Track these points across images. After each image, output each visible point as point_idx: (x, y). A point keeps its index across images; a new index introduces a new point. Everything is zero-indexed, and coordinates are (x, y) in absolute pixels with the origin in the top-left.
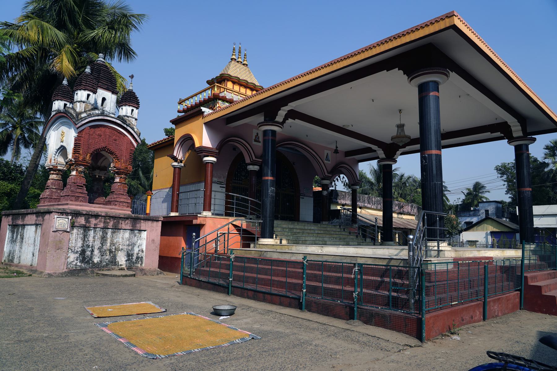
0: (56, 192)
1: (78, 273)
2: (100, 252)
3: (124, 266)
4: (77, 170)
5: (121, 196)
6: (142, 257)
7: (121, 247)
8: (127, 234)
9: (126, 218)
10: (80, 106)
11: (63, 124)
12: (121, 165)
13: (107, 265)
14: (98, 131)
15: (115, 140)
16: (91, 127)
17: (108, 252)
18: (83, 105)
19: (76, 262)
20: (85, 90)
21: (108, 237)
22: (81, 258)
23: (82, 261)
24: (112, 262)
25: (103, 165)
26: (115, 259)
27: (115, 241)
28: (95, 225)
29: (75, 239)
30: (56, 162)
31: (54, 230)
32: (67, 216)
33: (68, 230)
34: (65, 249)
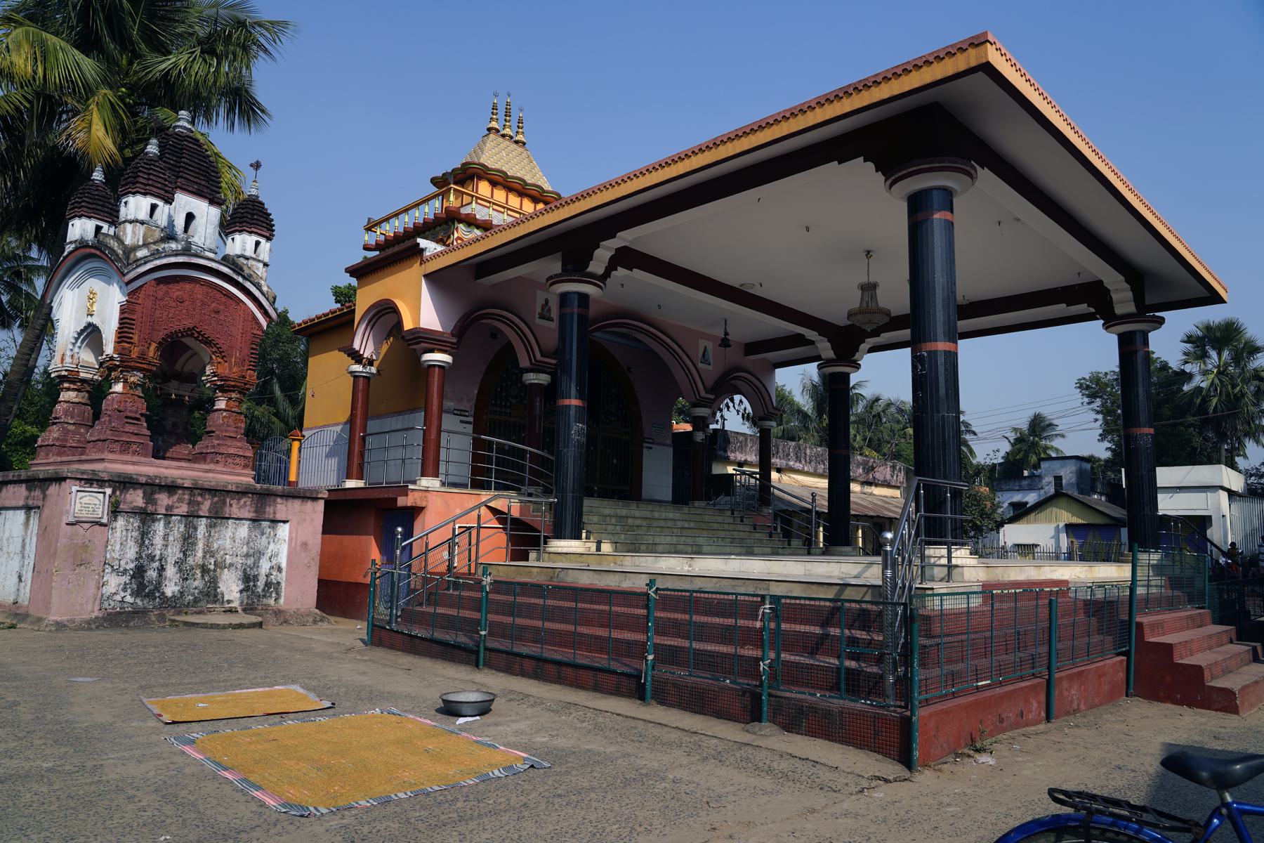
0: (74, 433)
1: (127, 621)
2: (180, 570)
3: (236, 604)
4: (126, 381)
5: (229, 442)
6: (279, 583)
7: (229, 560)
8: (243, 530)
9: (241, 493)
10: (134, 232)
11: (93, 273)
12: (230, 369)
13: (196, 601)
14: (176, 291)
15: (217, 312)
16: (160, 281)
17: (198, 572)
18: (141, 230)
19: (122, 594)
20: (145, 194)
21: (200, 536)
22: (135, 586)
23: (136, 594)
24: (208, 594)
25: (187, 369)
26: (216, 588)
27: (216, 546)
28: (169, 508)
29: (121, 542)
30: (76, 361)
31: (71, 519)
32: (101, 487)
33: (105, 520)
34: (96, 566)
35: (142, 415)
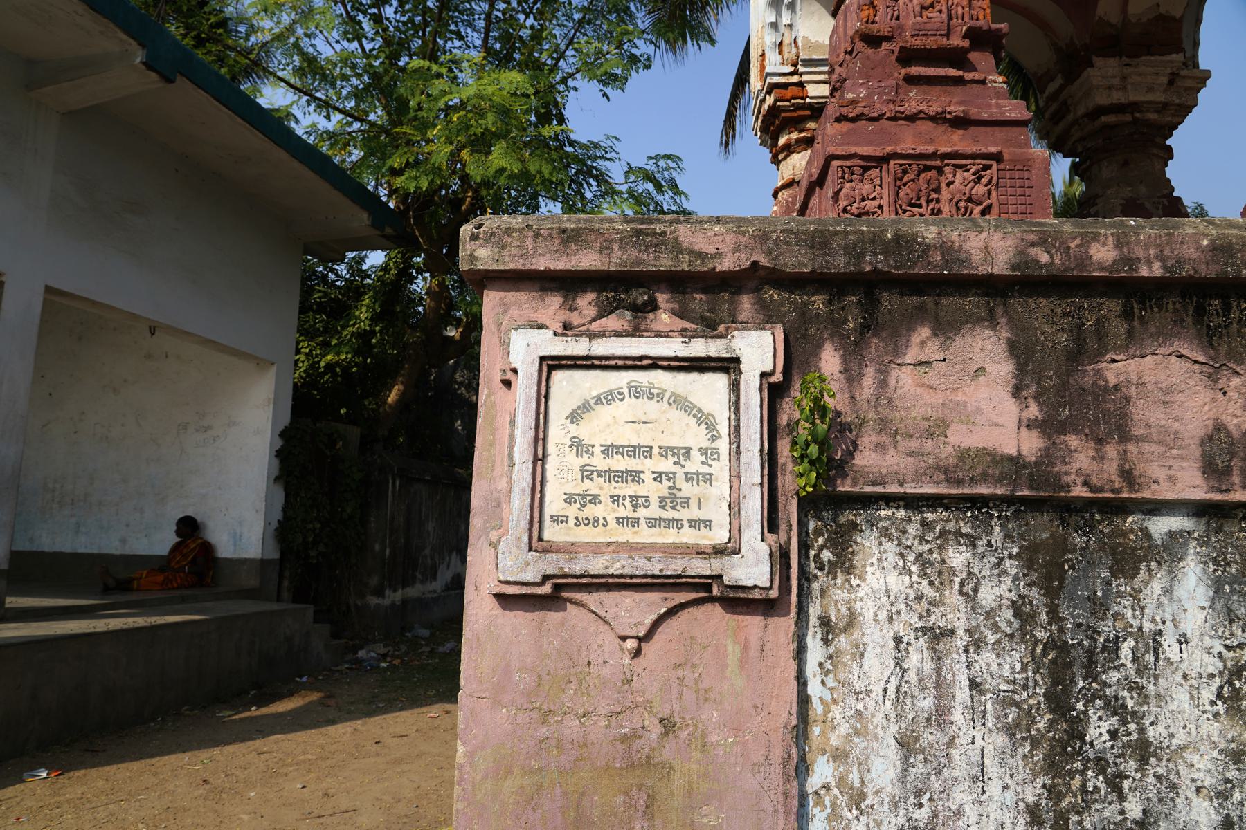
30: (789, 53)
31: (525, 569)
32: (710, 326)
33: (752, 568)
35: (979, 38)
